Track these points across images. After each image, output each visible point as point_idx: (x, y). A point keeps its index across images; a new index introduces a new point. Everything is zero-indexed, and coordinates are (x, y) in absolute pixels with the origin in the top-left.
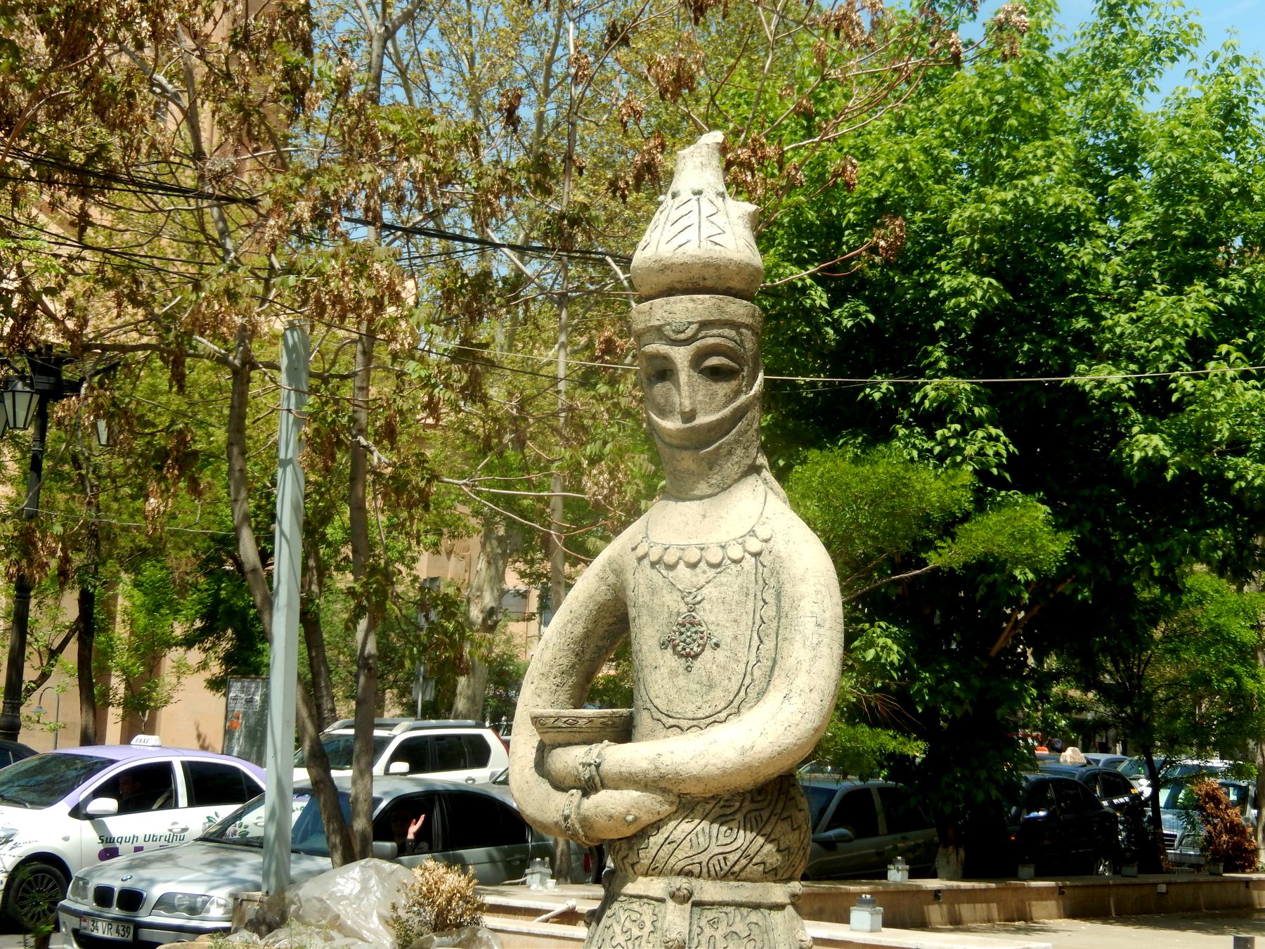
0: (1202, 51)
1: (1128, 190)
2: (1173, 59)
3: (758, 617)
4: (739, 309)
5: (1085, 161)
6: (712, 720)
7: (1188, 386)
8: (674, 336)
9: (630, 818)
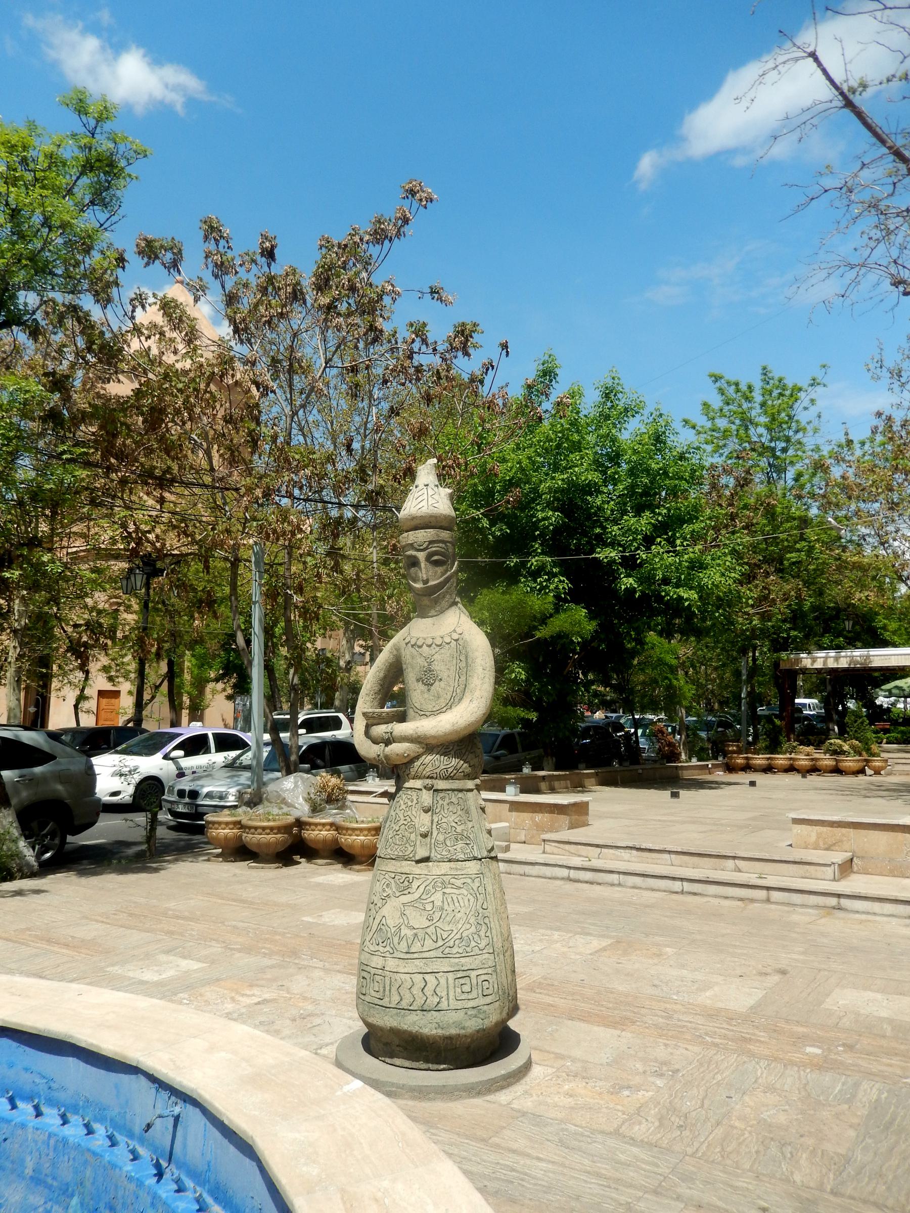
0: (646, 412)
1: (616, 473)
2: (633, 416)
4: (445, 535)
6: (440, 712)
7: (644, 556)
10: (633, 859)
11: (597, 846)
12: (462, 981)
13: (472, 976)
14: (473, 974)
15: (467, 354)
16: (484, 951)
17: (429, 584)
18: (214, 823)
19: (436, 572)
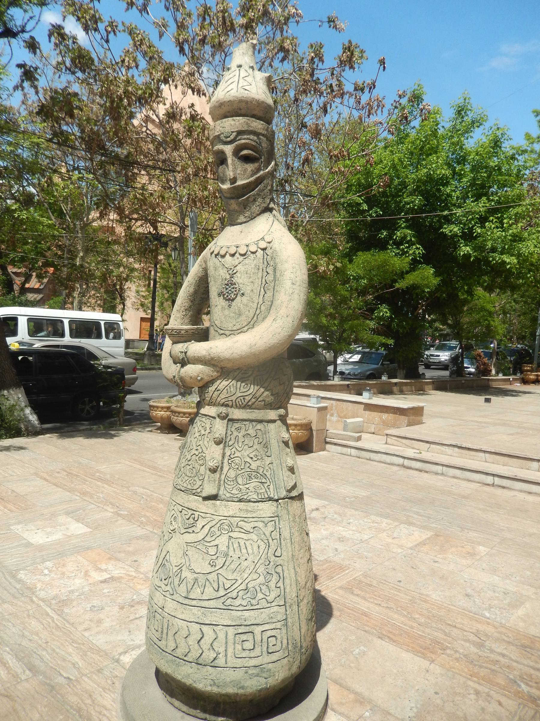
1: (462, 170)
2: (478, 127)
3: (264, 280)
5: (449, 163)
6: (240, 331)
7: (479, 231)
8: (225, 140)
9: (199, 378)
10: (455, 454)
11: (427, 442)
12: (244, 637)
13: (256, 632)
14: (258, 630)
15: (352, 67)
16: (273, 604)
17: (237, 184)
18: (154, 407)
19: (245, 170)
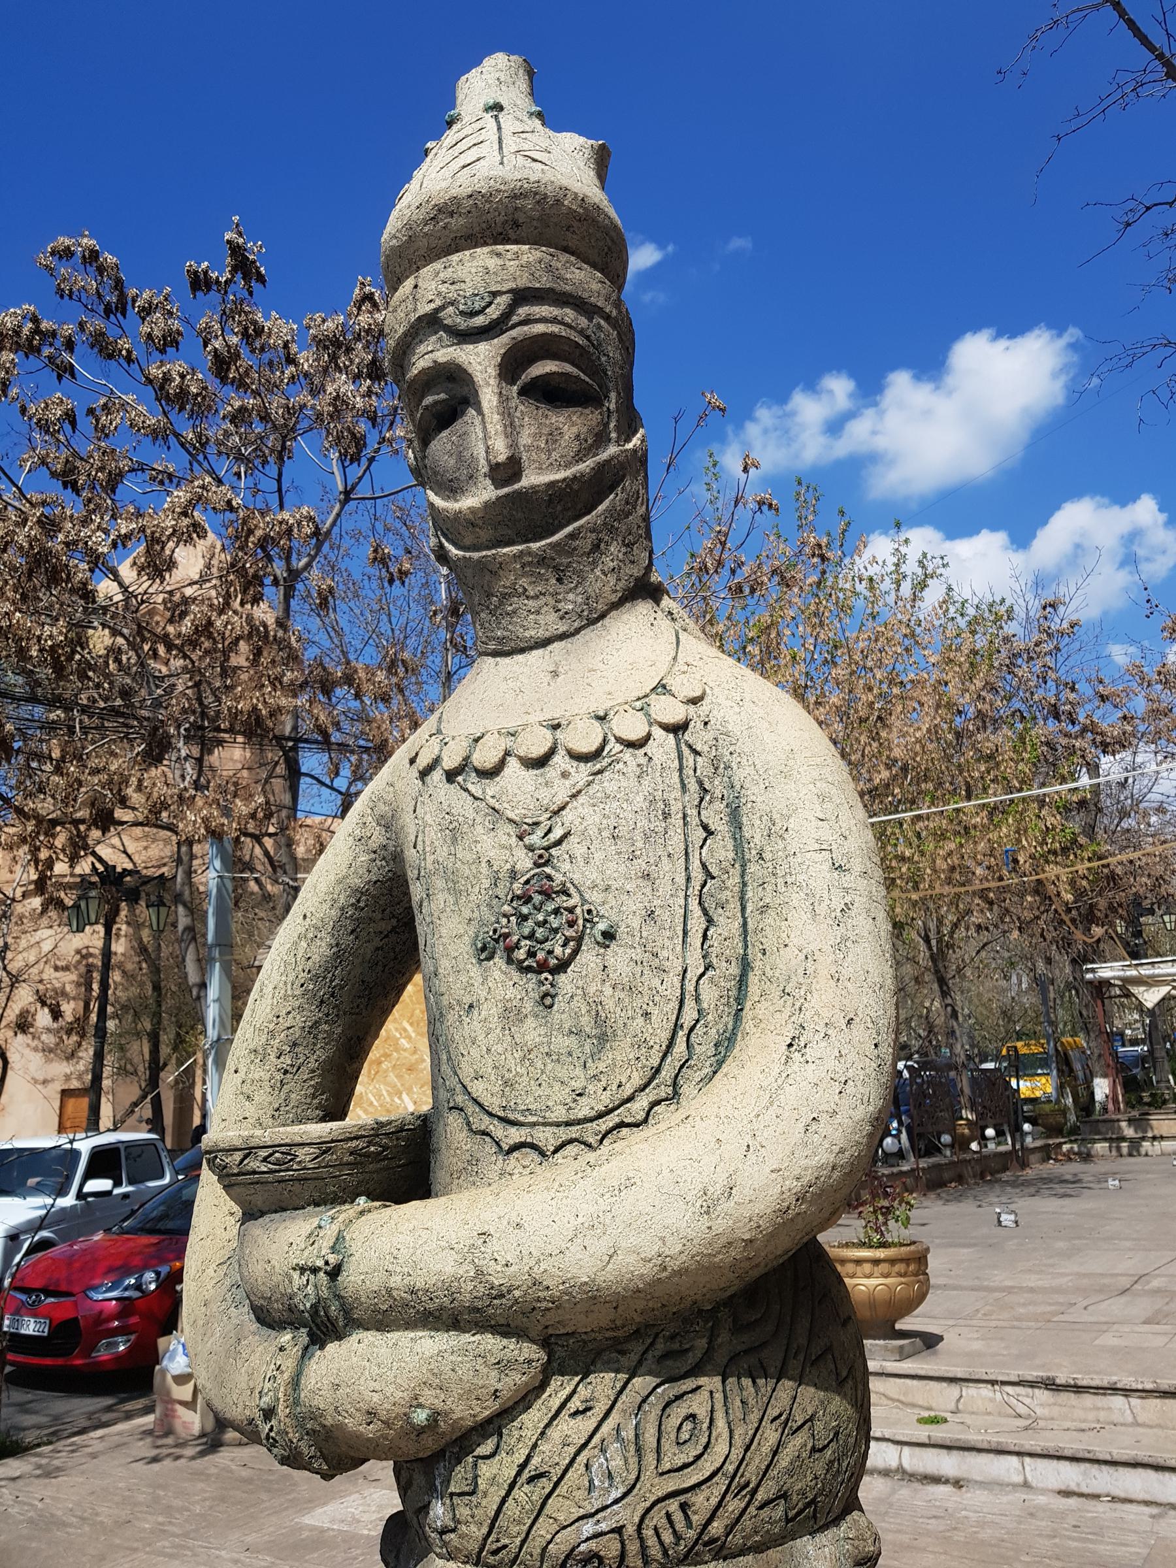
3: (695, 865)
8: (462, 323)
9: (420, 1417)
19: (553, 436)
